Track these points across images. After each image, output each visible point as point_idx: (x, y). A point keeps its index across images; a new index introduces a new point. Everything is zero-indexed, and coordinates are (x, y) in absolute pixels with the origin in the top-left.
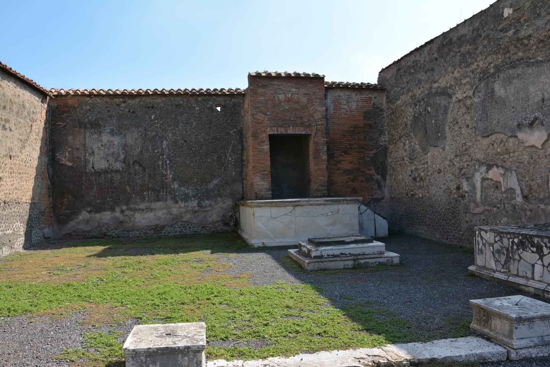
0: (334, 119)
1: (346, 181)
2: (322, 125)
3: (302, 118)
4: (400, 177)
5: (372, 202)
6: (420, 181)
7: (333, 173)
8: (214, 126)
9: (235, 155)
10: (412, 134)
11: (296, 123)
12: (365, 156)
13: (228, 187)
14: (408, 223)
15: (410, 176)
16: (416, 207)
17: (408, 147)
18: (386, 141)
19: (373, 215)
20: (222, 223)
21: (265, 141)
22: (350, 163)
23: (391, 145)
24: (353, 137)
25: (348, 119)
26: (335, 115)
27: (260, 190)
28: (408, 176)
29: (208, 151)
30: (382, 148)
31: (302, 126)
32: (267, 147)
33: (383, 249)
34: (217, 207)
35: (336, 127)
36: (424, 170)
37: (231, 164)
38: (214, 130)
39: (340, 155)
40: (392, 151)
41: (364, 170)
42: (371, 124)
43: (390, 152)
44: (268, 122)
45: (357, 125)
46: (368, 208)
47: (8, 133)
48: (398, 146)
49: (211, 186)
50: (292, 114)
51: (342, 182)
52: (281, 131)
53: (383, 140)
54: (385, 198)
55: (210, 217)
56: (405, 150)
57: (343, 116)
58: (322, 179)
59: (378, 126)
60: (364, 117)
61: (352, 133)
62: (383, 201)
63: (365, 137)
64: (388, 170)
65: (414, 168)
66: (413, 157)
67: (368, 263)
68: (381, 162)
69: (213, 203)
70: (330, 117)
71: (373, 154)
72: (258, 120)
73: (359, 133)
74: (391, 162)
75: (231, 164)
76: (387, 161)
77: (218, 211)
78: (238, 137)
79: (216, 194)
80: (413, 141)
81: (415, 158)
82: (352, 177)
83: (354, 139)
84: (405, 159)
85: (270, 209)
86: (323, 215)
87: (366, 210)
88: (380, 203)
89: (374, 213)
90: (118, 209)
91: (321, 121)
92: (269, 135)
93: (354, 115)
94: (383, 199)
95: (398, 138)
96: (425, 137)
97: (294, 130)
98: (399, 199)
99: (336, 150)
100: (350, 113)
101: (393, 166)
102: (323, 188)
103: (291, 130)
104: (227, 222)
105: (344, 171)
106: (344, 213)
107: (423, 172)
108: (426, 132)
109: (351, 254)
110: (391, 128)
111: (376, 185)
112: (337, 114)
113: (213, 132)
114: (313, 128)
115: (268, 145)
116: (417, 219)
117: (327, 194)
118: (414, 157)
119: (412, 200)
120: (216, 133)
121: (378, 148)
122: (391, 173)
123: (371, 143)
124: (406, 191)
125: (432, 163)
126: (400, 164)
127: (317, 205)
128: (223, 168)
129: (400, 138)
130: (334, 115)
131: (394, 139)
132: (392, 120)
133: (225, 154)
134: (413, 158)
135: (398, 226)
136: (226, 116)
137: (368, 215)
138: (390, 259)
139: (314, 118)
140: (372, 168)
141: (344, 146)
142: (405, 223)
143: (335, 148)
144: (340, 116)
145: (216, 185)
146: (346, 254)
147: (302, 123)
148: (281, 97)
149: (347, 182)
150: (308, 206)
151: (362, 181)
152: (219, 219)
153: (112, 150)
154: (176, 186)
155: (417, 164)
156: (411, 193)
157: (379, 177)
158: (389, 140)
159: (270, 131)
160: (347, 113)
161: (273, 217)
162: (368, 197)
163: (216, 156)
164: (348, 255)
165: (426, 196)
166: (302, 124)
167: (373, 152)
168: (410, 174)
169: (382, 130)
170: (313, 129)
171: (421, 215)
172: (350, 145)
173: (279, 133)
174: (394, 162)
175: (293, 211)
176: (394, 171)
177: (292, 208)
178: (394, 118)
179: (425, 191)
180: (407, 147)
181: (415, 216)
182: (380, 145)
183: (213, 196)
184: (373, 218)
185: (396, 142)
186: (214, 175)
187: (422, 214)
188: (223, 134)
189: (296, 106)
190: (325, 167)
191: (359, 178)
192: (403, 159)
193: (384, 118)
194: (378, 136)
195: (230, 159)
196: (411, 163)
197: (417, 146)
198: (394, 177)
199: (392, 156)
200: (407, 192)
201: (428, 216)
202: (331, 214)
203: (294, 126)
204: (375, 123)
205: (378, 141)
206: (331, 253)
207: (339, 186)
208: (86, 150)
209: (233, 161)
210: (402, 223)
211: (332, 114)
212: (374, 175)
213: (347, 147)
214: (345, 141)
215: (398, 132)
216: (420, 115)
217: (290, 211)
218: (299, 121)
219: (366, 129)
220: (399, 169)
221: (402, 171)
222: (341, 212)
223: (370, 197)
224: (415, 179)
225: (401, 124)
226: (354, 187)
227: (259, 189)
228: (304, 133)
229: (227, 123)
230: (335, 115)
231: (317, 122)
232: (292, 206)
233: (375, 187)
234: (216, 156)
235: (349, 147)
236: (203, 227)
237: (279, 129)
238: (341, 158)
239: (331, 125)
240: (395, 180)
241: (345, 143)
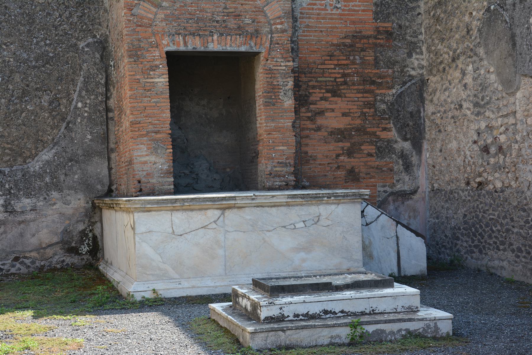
0: (310, 18)
1: (334, 156)
2: (283, 31)
3: (239, 15)
4: (454, 145)
5: (390, 198)
6: (496, 154)
7: (307, 137)
8: (39, 30)
9: (92, 97)
10: (481, 51)
11: (226, 27)
12: (375, 100)
13: (75, 168)
14: (470, 246)
15: (475, 142)
16: (488, 210)
17: (471, 80)
18: (422, 67)
19: (394, 227)
20: (61, 249)
21: (157, 67)
22: (344, 115)
23: (435, 76)
24: (351, 58)
25: (342, 19)
26: (313, 9)
27: (147, 174)
28: (471, 143)
29: (28, 86)
30: (413, 81)
31: (240, 35)
32: (163, 80)
33: (416, 302)
34: (50, 212)
35: (314, 36)
36: (507, 129)
37: (83, 118)
38: (39, 39)
39: (322, 99)
40: (436, 90)
41: (375, 129)
42: (389, 29)
43: (430, 90)
44: (164, 24)
45: (360, 32)
46: (382, 213)
48: (449, 77)
49: (35, 166)
50: (217, 7)
51: (327, 157)
53: (416, 65)
54: (419, 190)
55: (34, 235)
56: (465, 85)
57: (329, 12)
58: (283, 151)
59: (406, 34)
60: (376, 13)
61: (349, 49)
62: (416, 197)
63: (376, 58)
64: (427, 129)
65: (483, 125)
66: (482, 100)
67: (383, 331)
68: (411, 113)
69: (41, 203)
70: (301, 13)
71: (393, 95)
72: (142, 18)
73: (363, 50)
74: (433, 113)
75: (83, 118)
76: (424, 110)
77: (53, 221)
78: (98, 56)
79: (47, 183)
80: (483, 66)
81: (488, 103)
82: (347, 145)
83: (353, 63)
84: (465, 105)
85: (170, 215)
86: (284, 227)
87: (378, 217)
88: (410, 202)
89: (394, 223)
91: (282, 23)
92: (167, 53)
93: (354, 10)
94: (414, 192)
95: (450, 60)
96: (510, 55)
97: (223, 43)
98: (451, 192)
99: (314, 87)
100: (345, 6)
101: (438, 121)
102: (285, 169)
103: (216, 42)
104: (73, 245)
105: (331, 132)
106: (330, 223)
107: (504, 133)
108: (514, 45)
109: (345, 312)
110: (434, 37)
111: (401, 162)
112: (315, 7)
113: (37, 43)
114: (264, 39)
115: (164, 76)
116: (490, 237)
117: (293, 183)
118: (485, 101)
119: (479, 195)
120: (46, 45)
121: (405, 83)
122: (433, 136)
123: (390, 71)
124: (466, 175)
125: (526, 113)
126: (453, 117)
127: (272, 206)
128: (64, 125)
129: (453, 60)
130: (309, 9)
131: (441, 62)
132: (438, 20)
133: (68, 94)
134: (483, 103)
135: (448, 251)
136: (67, 7)
137: (383, 227)
138: (432, 324)
139: (266, 16)
140: (392, 125)
141: (332, 79)
142: (465, 244)
143: (311, 84)
144: (323, 12)
145: (48, 162)
146: (335, 313)
147: (239, 28)
149: (338, 156)
150: (253, 209)
151: (370, 155)
152: (55, 239)
155: (492, 116)
156: (478, 180)
157: (407, 145)
158: (430, 65)
159: (168, 45)
160: (339, 6)
161: (178, 231)
162: (382, 189)
163: (47, 98)
164: (338, 315)
165: (510, 186)
166: (240, 30)
167: (394, 91)
168: (475, 138)
169: (415, 43)
170: (263, 42)
171: (499, 227)
172: (344, 75)
173: (190, 48)
174: (439, 112)
175: (221, 218)
176: (440, 131)
177: (217, 213)
178: (442, 15)
179: (509, 175)
180: (469, 80)
181: (486, 229)
182: (410, 76)
183: (40, 188)
184: (393, 234)
185: (444, 69)
186: (42, 141)
187: (502, 225)
188: (61, 47)
190: (291, 124)
191: (363, 147)
192: (461, 106)
193: (420, 16)
194: (405, 55)
195: (80, 105)
196: (478, 114)
197: (493, 77)
198: (438, 145)
199: (435, 99)
200: (467, 178)
201: (515, 230)
202: (302, 225)
203: (222, 35)
204: (400, 27)
205: (405, 66)
206: (302, 310)
207: (320, 164)
209: (86, 109)
210: (456, 244)
211: (304, 8)
212: (396, 142)
213: (338, 80)
214: (333, 66)
215: (449, 47)
216: (502, 7)
217: (212, 220)
218: (232, 23)
219: (379, 41)
220: (449, 128)
221: (457, 132)
222: (323, 222)
223: (387, 189)
224: (486, 149)
225: (458, 27)
226: (352, 168)
227: (145, 173)
228: (243, 49)
229: (71, 24)
230: (313, 9)
231: (271, 25)
232: (217, 209)
233: (399, 166)
234: (47, 98)
235: (342, 80)
236: (16, 259)
237: (189, 39)
238: (324, 105)
239: (304, 32)
240: (441, 151)
241: (333, 71)
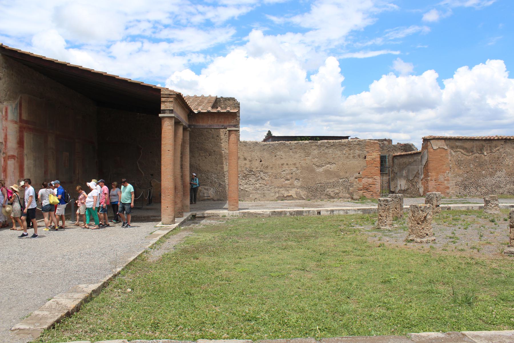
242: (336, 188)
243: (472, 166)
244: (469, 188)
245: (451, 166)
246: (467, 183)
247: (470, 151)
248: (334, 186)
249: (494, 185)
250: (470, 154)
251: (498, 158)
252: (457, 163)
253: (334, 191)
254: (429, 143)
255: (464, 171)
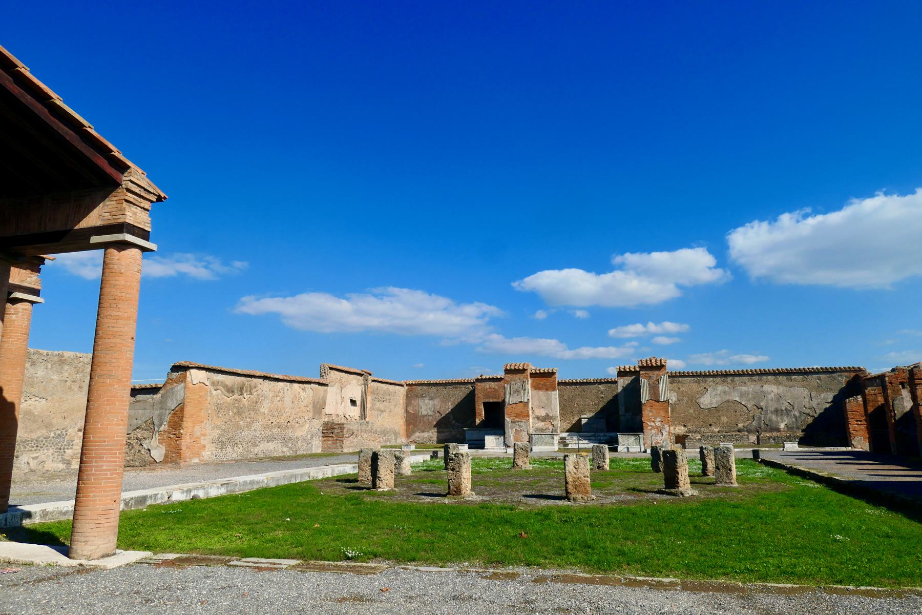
47: (390, 403)
52: (487, 400)
90: (430, 431)
148: (488, 386)
153: (429, 407)
154: (454, 422)
189: (493, 390)
208: (419, 407)
218: (494, 396)
242: (42, 451)
243: (231, 413)
244: (226, 448)
245: (209, 412)
246: (224, 440)
247: (230, 390)
248: (37, 446)
249: (250, 442)
250: (231, 395)
251: (257, 402)
252: (216, 408)
253: (37, 457)
254: (188, 373)
255: (223, 421)
